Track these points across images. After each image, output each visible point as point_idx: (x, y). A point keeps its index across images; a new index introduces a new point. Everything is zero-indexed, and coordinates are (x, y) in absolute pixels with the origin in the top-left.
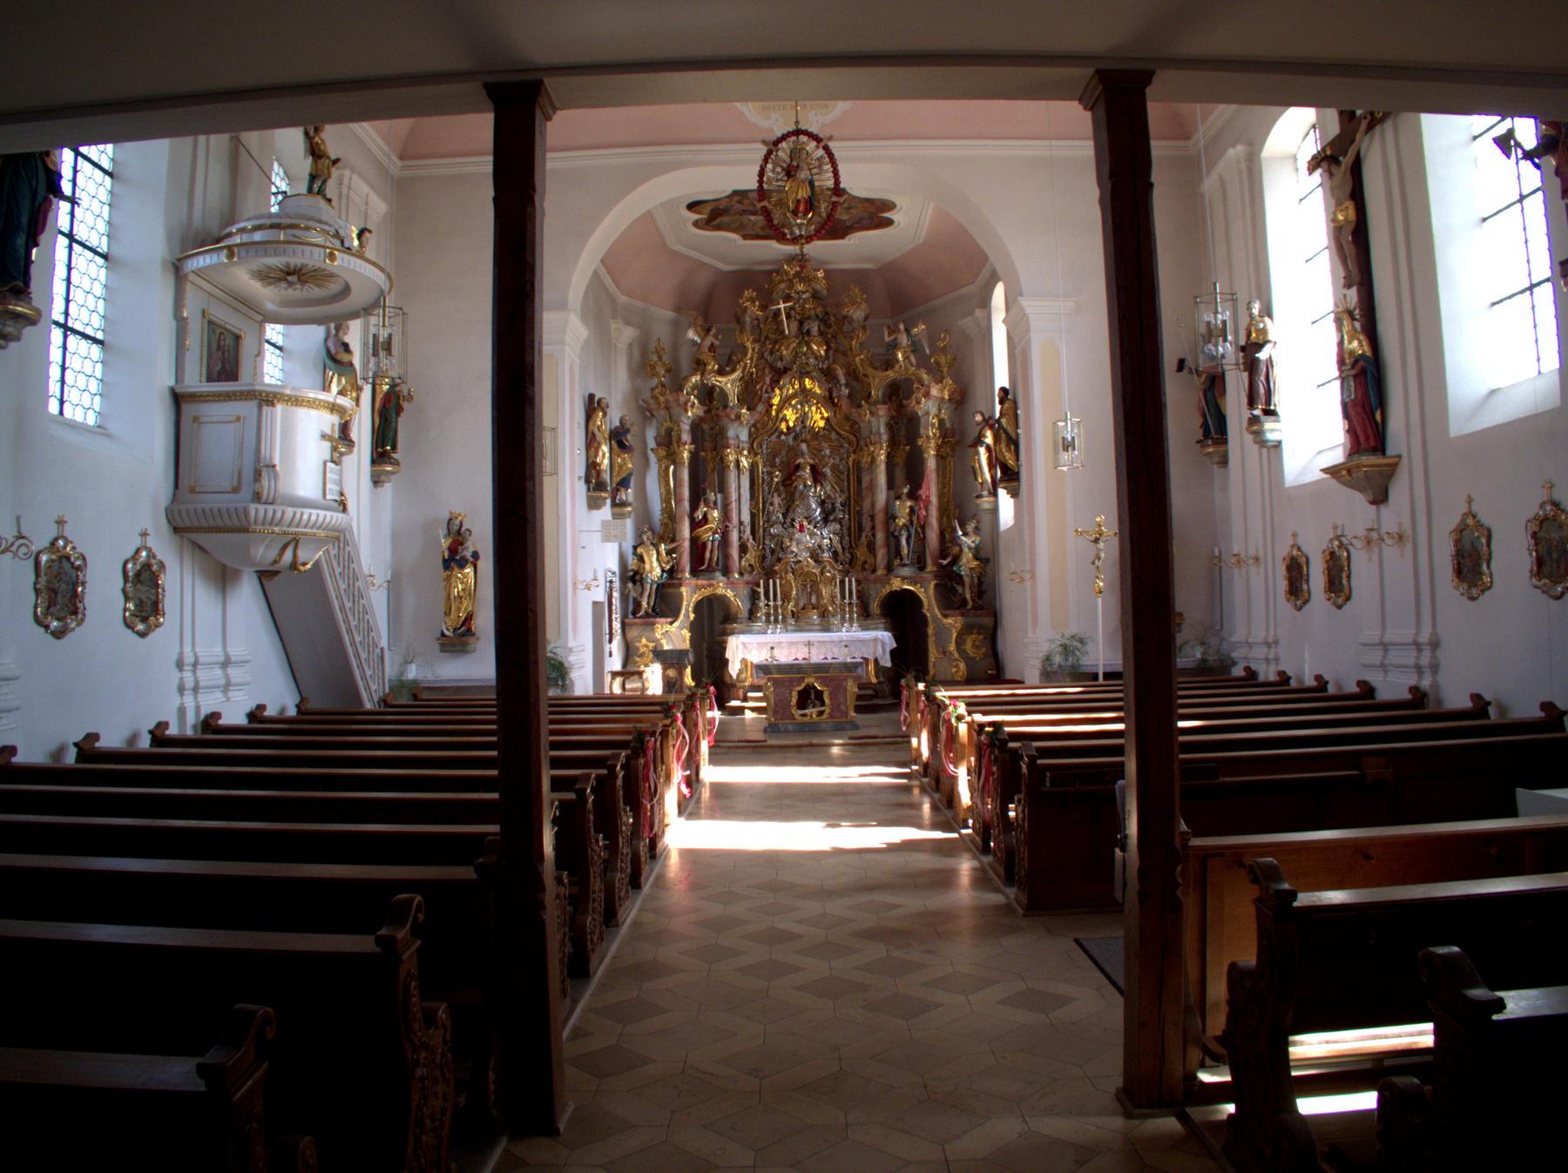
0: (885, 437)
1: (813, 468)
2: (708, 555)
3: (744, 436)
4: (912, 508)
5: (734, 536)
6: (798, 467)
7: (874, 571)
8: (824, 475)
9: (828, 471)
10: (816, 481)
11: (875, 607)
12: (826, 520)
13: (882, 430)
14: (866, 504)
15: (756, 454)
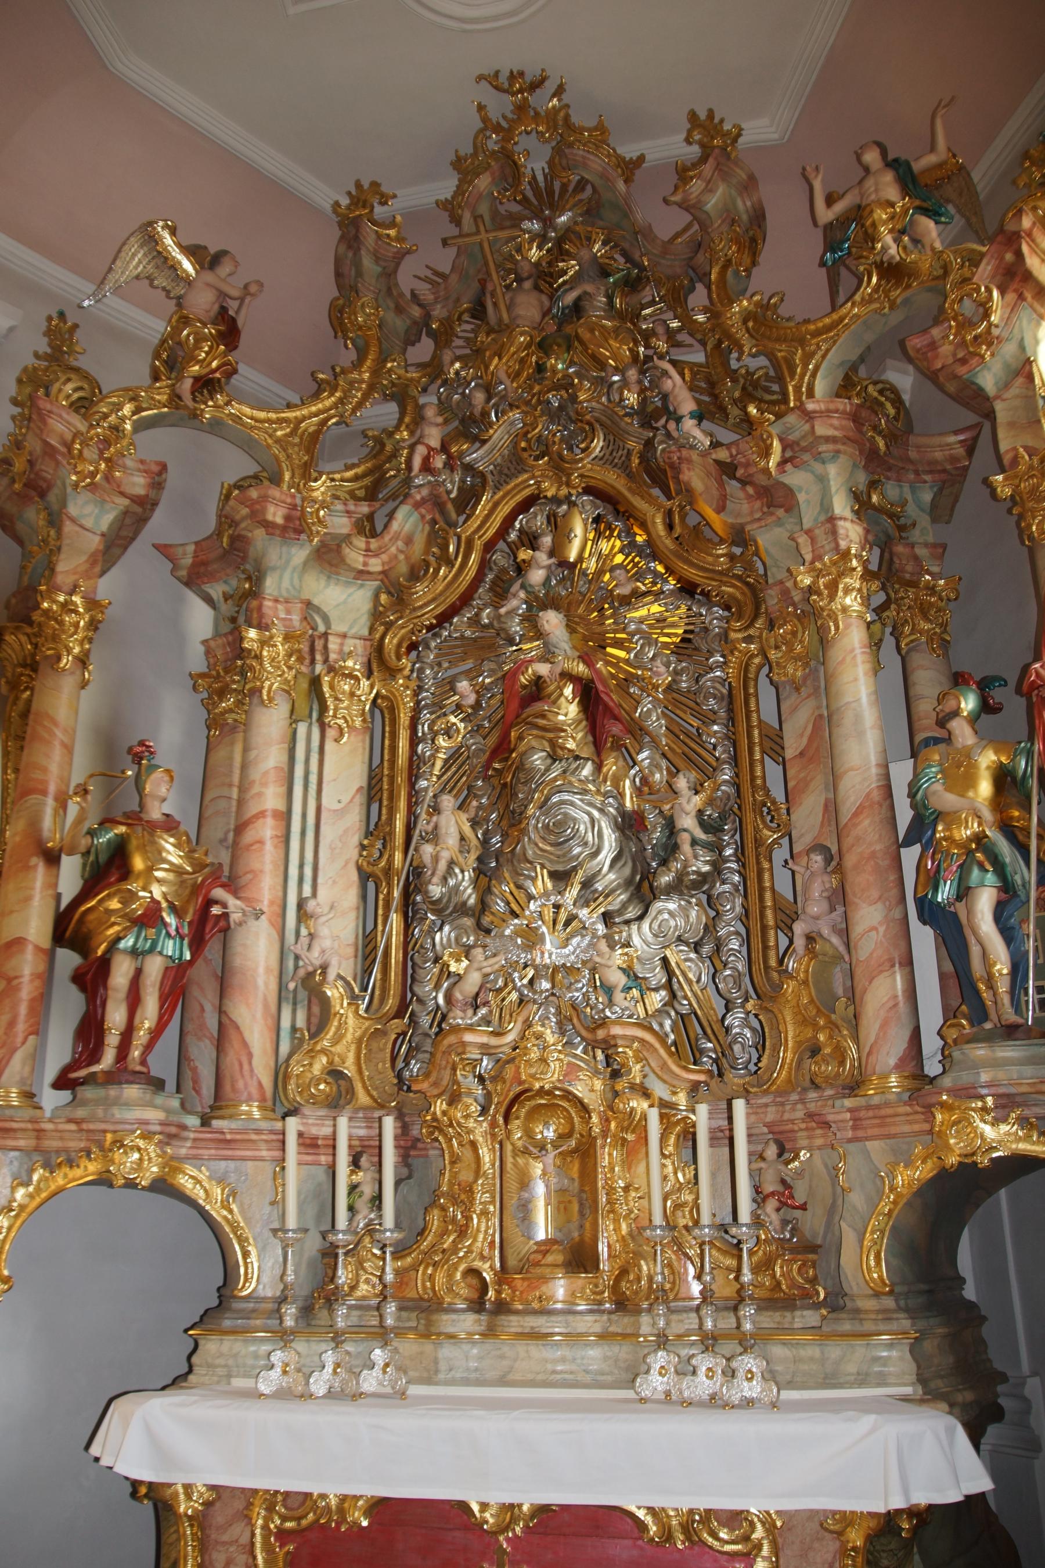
0: (851, 533)
1: (589, 696)
2: (116, 1016)
3: (346, 606)
4: (1003, 778)
5: (257, 950)
6: (537, 690)
7: (854, 1086)
8: (638, 731)
9: (651, 714)
10: (599, 742)
11: (867, 1261)
12: (643, 891)
13: (841, 505)
14: (807, 818)
15: (391, 673)
